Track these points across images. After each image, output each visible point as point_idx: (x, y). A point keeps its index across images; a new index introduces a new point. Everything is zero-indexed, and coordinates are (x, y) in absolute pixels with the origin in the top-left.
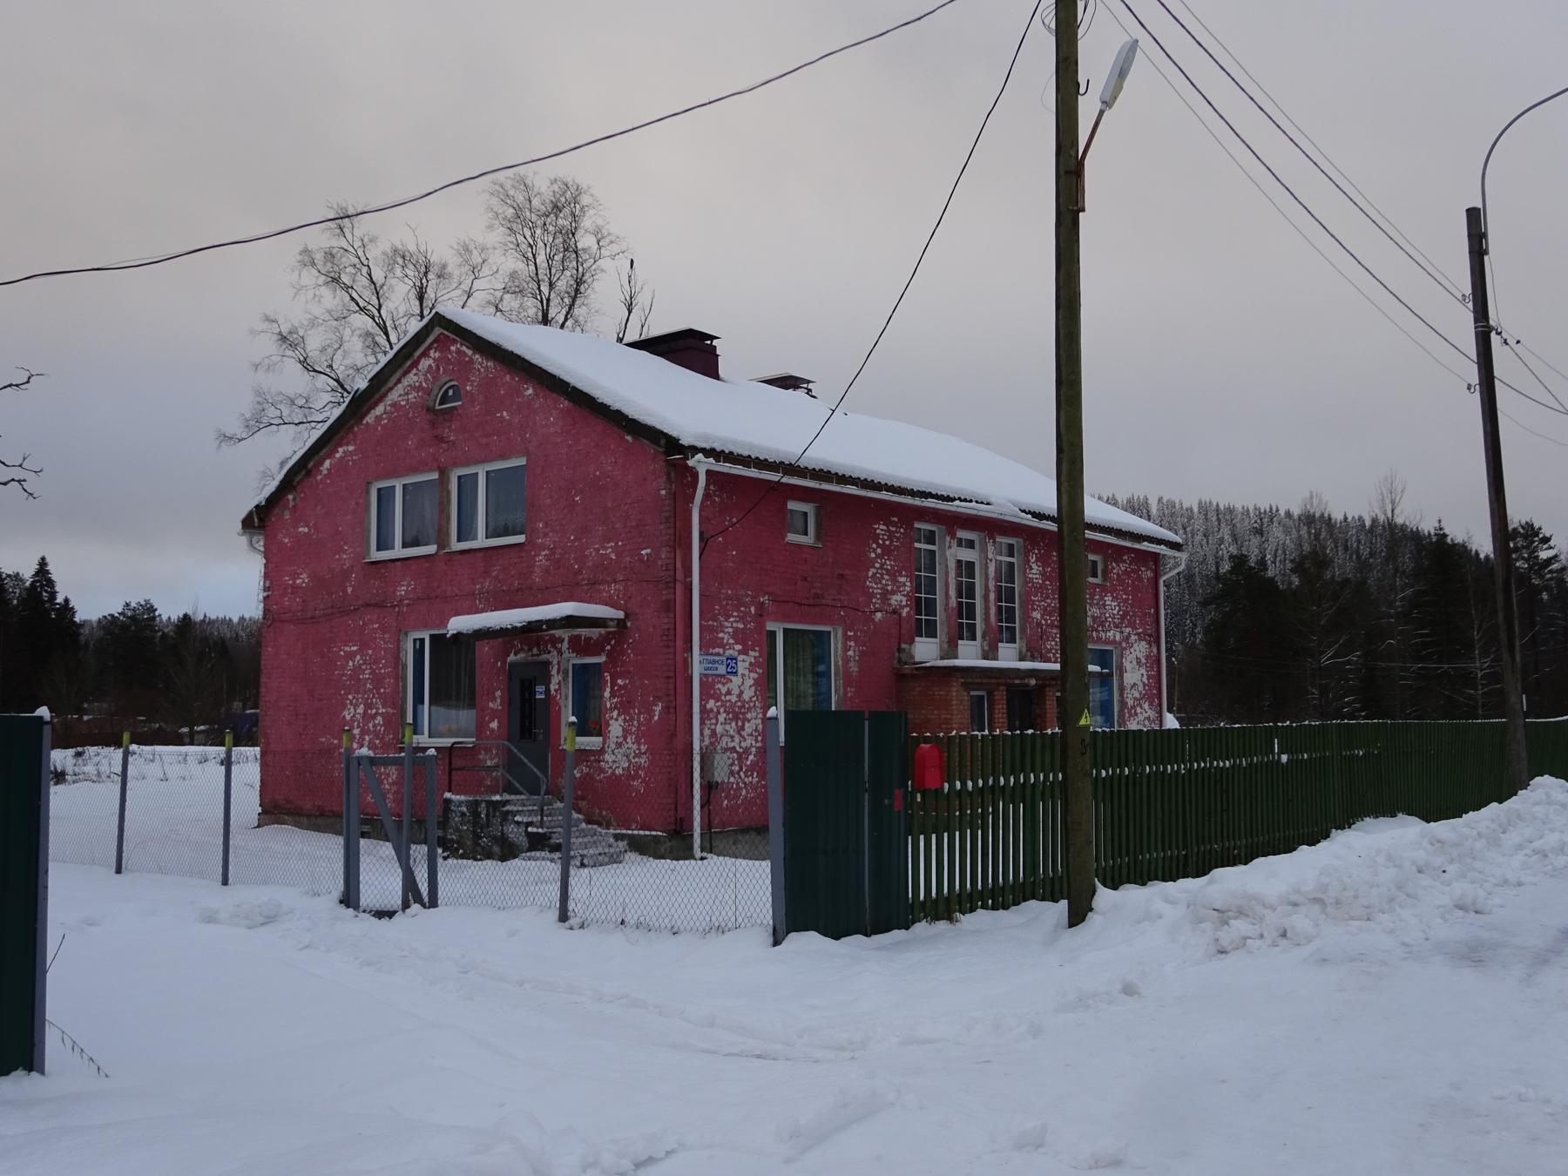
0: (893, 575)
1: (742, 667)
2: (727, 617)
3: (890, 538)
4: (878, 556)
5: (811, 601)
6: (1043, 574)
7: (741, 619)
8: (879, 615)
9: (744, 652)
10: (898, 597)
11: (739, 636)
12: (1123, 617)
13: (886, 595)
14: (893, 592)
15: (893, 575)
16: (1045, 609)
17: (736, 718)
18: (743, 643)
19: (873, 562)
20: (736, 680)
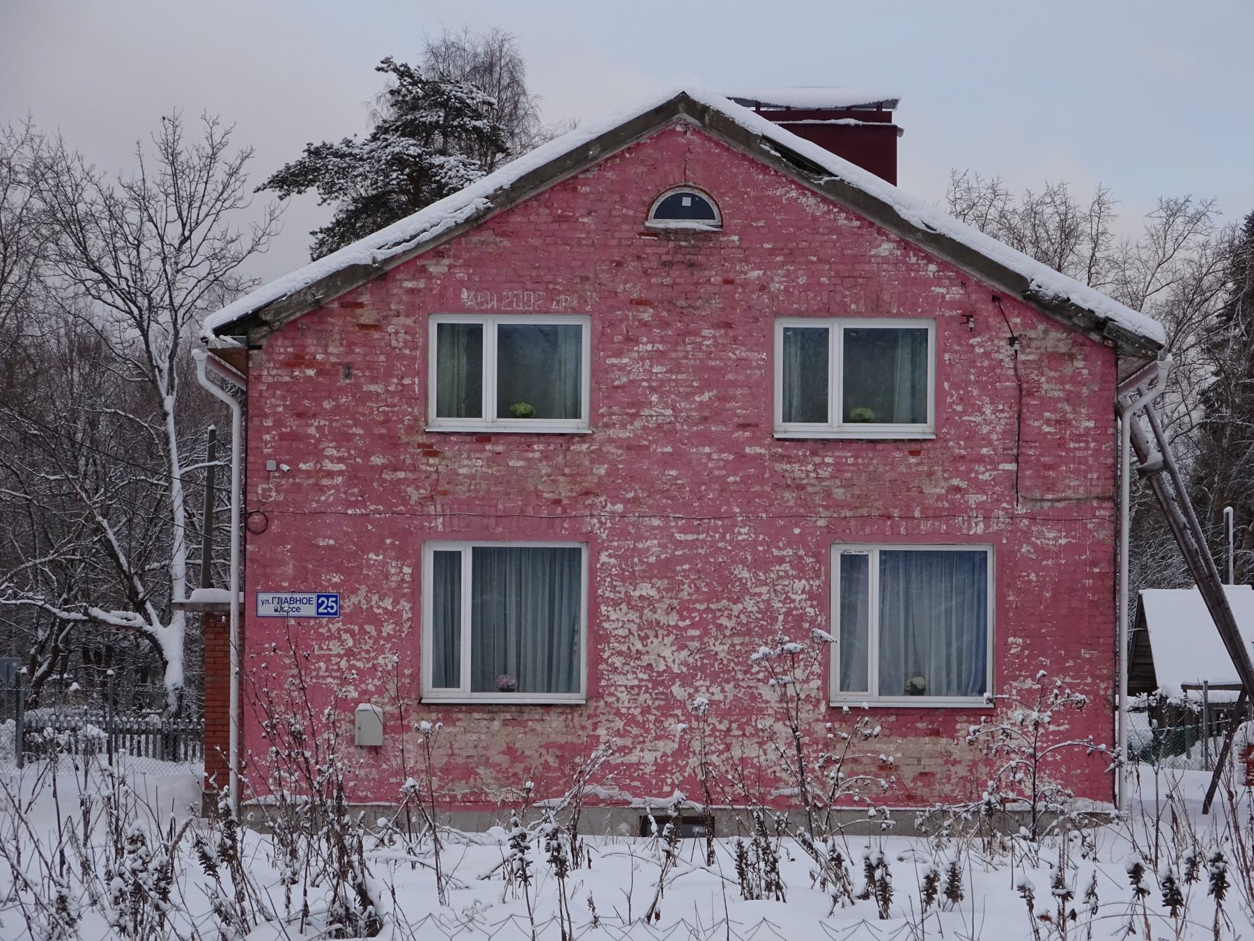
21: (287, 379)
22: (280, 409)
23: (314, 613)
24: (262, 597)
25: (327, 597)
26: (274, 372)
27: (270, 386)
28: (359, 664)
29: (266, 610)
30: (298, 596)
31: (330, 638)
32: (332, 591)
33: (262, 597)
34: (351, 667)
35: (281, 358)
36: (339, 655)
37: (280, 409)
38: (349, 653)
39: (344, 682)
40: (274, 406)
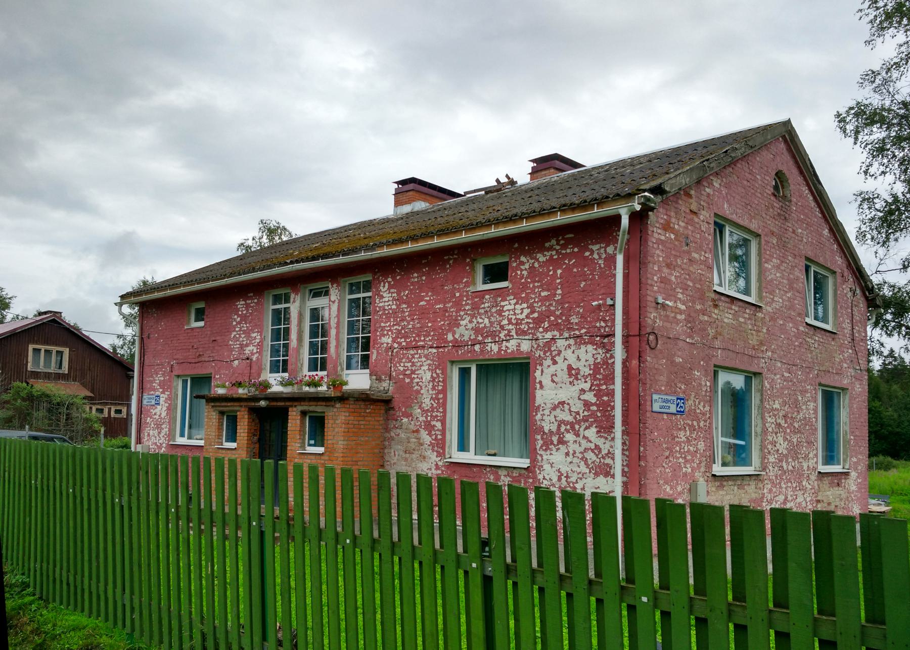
0: (247, 333)
1: (162, 400)
2: (157, 374)
3: (247, 309)
4: (239, 323)
5: (197, 360)
6: (399, 300)
7: (163, 375)
8: (236, 362)
9: (163, 393)
10: (251, 348)
11: (162, 385)
12: (538, 322)
13: (242, 347)
14: (247, 345)
15: (247, 333)
16: (399, 332)
17: (158, 428)
18: (163, 388)
19: (235, 327)
20: (159, 407)
21: (663, 238)
22: (661, 259)
23: (675, 412)
24: (655, 397)
25: (681, 399)
26: (659, 231)
27: (660, 242)
28: (691, 448)
29: (656, 407)
30: (669, 398)
31: (680, 429)
32: (681, 396)
33: (655, 397)
34: (689, 451)
35: (662, 221)
36: (683, 442)
37: (661, 259)
38: (688, 441)
39: (686, 461)
40: (659, 256)
